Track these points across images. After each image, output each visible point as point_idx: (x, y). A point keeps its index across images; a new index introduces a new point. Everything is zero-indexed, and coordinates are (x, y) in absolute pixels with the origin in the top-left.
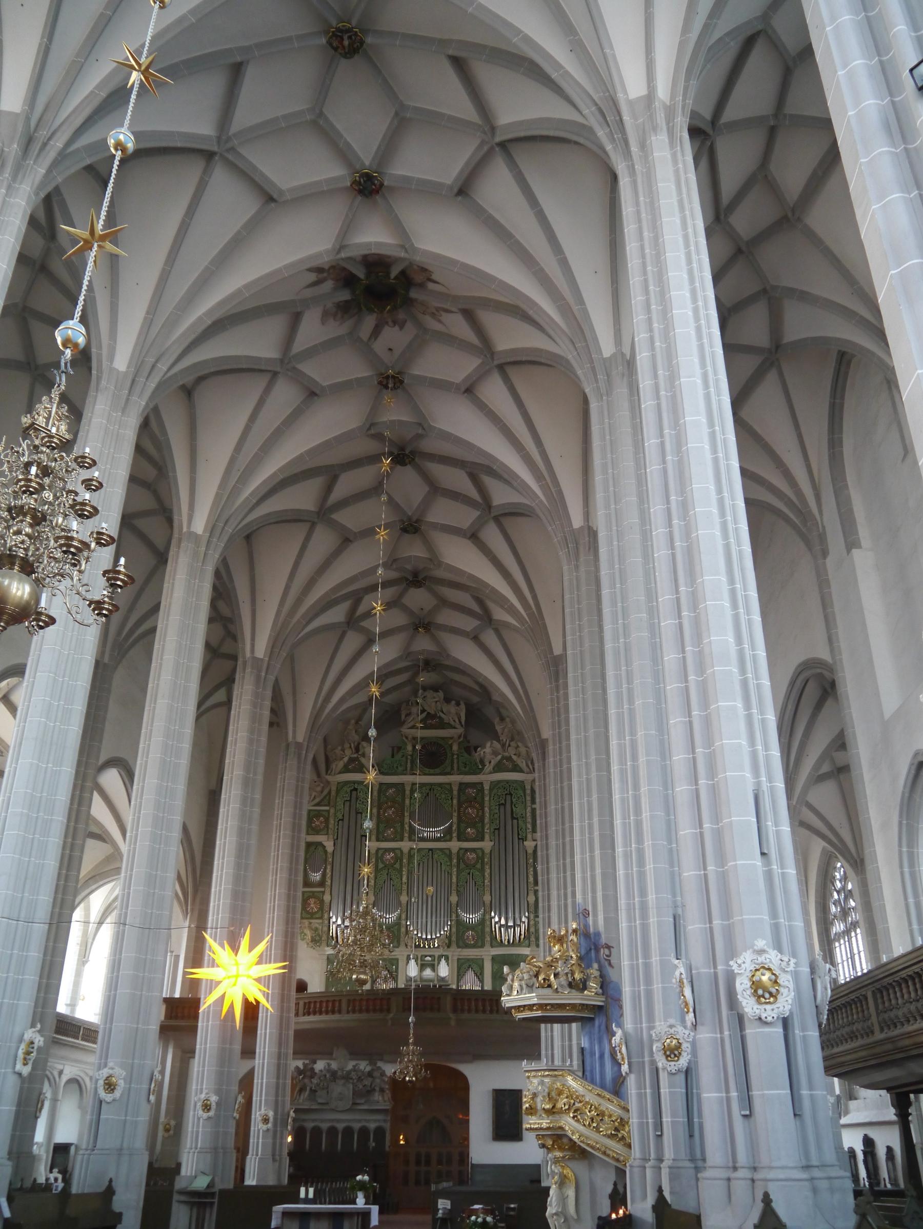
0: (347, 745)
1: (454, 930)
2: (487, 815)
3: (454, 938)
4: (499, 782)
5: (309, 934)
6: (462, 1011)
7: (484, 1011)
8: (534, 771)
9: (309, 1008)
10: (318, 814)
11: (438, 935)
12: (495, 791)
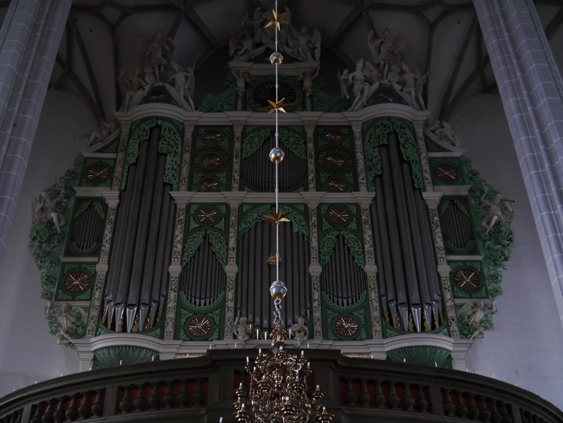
0: (148, 70)
1: (317, 314)
3: (318, 327)
5: (64, 322)
6: (360, 403)
7: (403, 407)
9: (42, 413)
10: (99, 165)
12: (371, 131)
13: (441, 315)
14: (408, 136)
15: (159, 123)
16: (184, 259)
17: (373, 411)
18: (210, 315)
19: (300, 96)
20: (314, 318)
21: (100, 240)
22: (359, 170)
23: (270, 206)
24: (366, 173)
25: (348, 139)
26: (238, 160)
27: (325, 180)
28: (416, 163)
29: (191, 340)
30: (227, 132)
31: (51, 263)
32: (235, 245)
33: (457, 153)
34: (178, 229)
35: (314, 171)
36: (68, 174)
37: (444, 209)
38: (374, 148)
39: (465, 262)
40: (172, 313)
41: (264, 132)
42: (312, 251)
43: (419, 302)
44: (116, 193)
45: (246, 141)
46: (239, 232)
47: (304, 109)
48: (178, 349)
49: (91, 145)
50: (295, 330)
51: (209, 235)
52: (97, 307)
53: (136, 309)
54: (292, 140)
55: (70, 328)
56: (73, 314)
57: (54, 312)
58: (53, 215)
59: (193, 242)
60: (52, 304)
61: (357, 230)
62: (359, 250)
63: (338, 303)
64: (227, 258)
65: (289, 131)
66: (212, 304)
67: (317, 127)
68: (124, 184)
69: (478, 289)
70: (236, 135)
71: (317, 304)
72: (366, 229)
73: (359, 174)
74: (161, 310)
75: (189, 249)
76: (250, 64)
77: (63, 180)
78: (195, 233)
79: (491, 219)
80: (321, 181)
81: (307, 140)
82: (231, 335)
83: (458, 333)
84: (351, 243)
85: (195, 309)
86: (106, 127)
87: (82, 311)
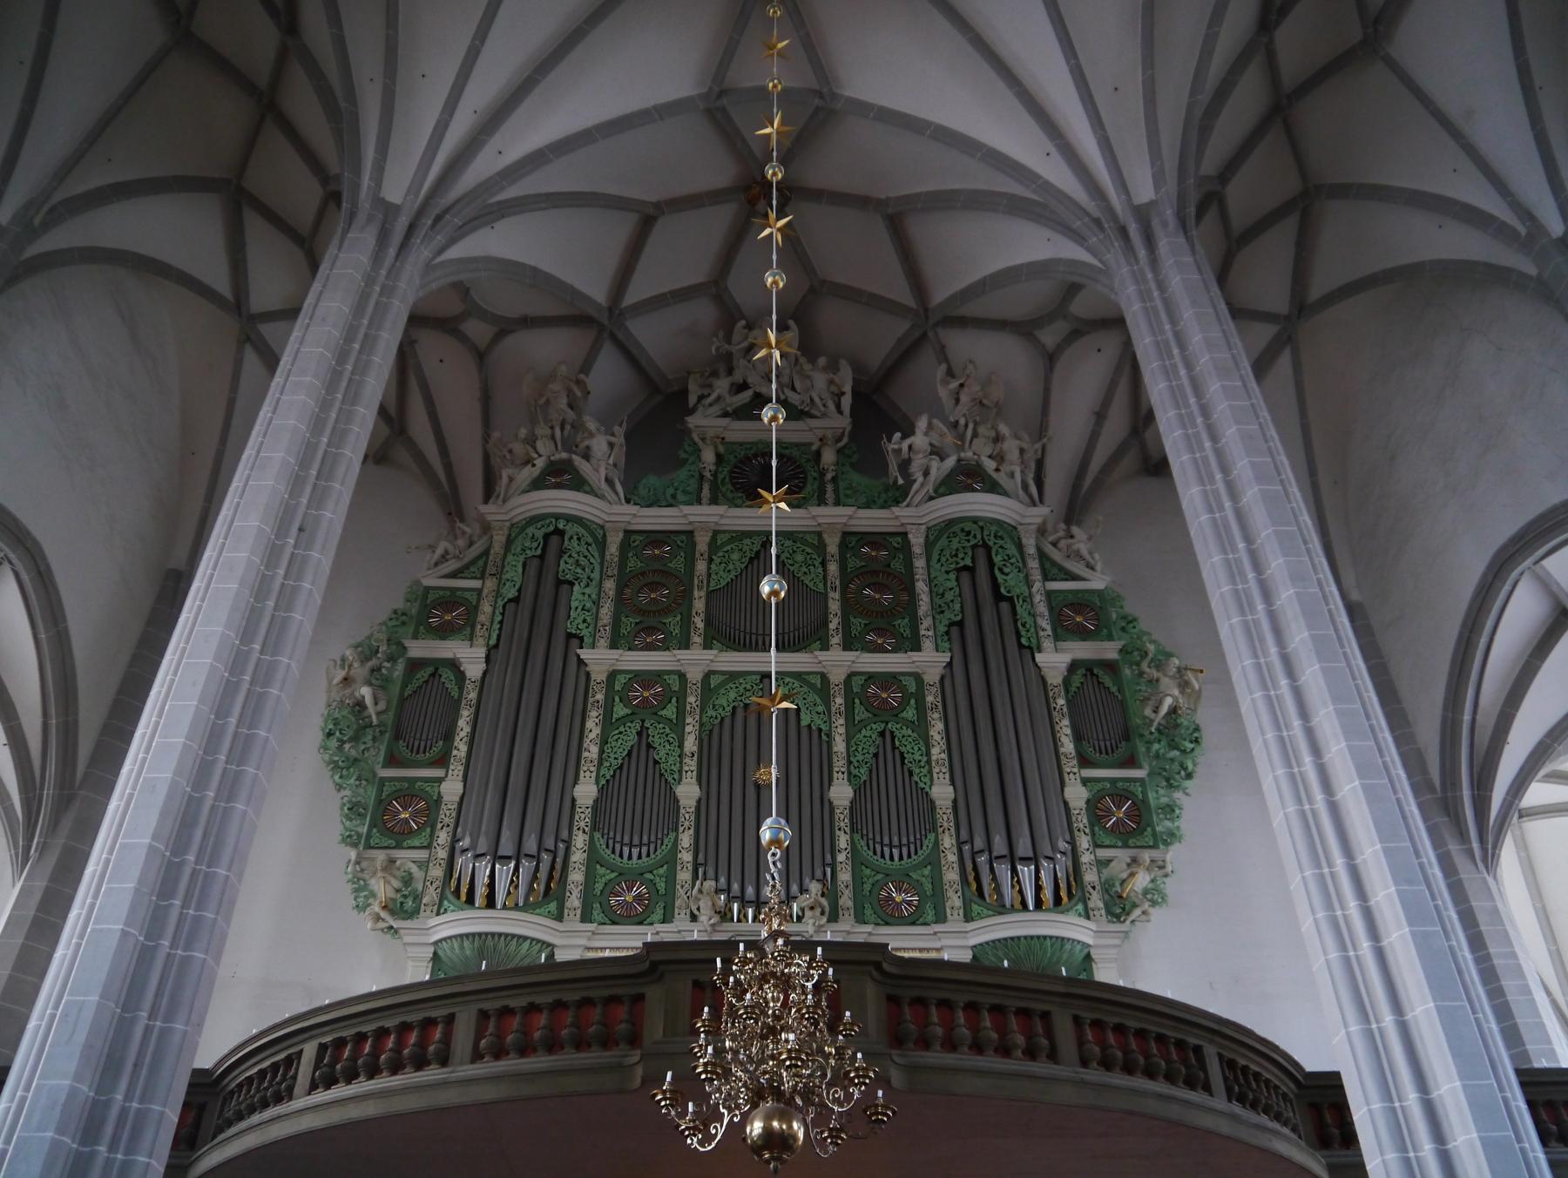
0: (542, 430)
1: (845, 876)
3: (846, 900)
4: (951, 523)
5: (382, 888)
6: (925, 1043)
7: (1005, 1051)
8: (1041, 501)
9: (336, 1059)
10: (450, 601)
12: (943, 542)
13: (1072, 879)
14: (1008, 552)
15: (561, 526)
17: (949, 1059)
19: (815, 479)
21: (449, 736)
23: (758, 677)
24: (934, 617)
25: (901, 556)
26: (703, 593)
28: (1024, 601)
29: (614, 923)
31: (359, 779)
32: (695, 749)
33: (1097, 582)
35: (839, 614)
36: (394, 616)
37: (1074, 685)
38: (947, 572)
39: (1113, 781)
42: (835, 760)
43: (1031, 854)
44: (481, 652)
45: (717, 560)
47: (822, 502)
48: (589, 939)
49: (436, 564)
50: (803, 905)
51: (648, 728)
52: (442, 862)
53: (512, 865)
54: (799, 558)
55: (392, 899)
56: (398, 873)
57: (362, 870)
58: (366, 692)
60: (358, 855)
63: (883, 856)
64: (680, 771)
65: (794, 542)
66: (652, 856)
67: (845, 534)
68: (494, 636)
69: (1139, 831)
70: (698, 548)
74: (558, 866)
75: (612, 756)
76: (726, 421)
77: (384, 628)
79: (1160, 702)
83: (1103, 912)
86: (464, 533)
87: (414, 869)
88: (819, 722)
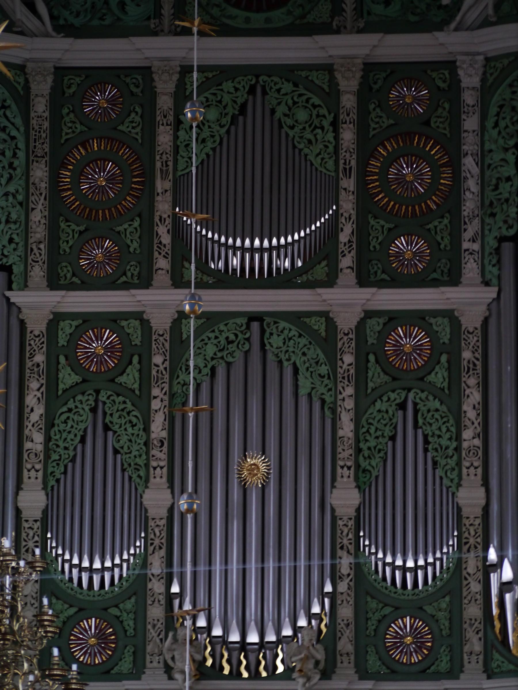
2: (473, 185)
11: (287, 632)
16: (50, 470)
18: (114, 611)
20: (339, 621)
22: (465, 213)
23: (244, 321)
24: (483, 221)
25: (447, 106)
26: (168, 185)
27: (380, 240)
30: (138, 87)
32: (164, 434)
34: (33, 390)
35: (354, 217)
40: (32, 609)
41: (232, 90)
42: (339, 450)
46: (174, 394)
51: (104, 403)
59: (69, 425)
61: (449, 389)
62: (448, 443)
64: (147, 465)
65: (296, 85)
71: (346, 587)
72: (469, 387)
73: (465, 223)
78: (72, 400)
80: (370, 244)
81: (341, 117)
82: (159, 662)
84: (431, 425)
85: (81, 597)
88: (323, 390)
